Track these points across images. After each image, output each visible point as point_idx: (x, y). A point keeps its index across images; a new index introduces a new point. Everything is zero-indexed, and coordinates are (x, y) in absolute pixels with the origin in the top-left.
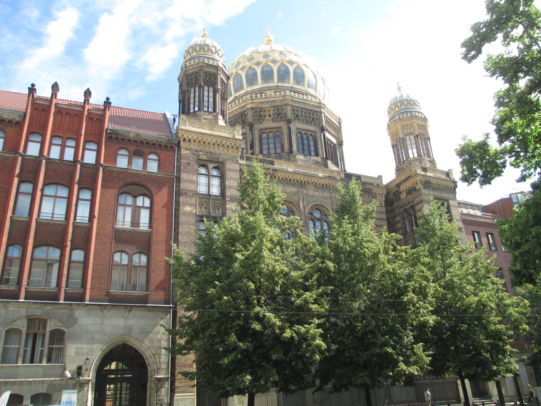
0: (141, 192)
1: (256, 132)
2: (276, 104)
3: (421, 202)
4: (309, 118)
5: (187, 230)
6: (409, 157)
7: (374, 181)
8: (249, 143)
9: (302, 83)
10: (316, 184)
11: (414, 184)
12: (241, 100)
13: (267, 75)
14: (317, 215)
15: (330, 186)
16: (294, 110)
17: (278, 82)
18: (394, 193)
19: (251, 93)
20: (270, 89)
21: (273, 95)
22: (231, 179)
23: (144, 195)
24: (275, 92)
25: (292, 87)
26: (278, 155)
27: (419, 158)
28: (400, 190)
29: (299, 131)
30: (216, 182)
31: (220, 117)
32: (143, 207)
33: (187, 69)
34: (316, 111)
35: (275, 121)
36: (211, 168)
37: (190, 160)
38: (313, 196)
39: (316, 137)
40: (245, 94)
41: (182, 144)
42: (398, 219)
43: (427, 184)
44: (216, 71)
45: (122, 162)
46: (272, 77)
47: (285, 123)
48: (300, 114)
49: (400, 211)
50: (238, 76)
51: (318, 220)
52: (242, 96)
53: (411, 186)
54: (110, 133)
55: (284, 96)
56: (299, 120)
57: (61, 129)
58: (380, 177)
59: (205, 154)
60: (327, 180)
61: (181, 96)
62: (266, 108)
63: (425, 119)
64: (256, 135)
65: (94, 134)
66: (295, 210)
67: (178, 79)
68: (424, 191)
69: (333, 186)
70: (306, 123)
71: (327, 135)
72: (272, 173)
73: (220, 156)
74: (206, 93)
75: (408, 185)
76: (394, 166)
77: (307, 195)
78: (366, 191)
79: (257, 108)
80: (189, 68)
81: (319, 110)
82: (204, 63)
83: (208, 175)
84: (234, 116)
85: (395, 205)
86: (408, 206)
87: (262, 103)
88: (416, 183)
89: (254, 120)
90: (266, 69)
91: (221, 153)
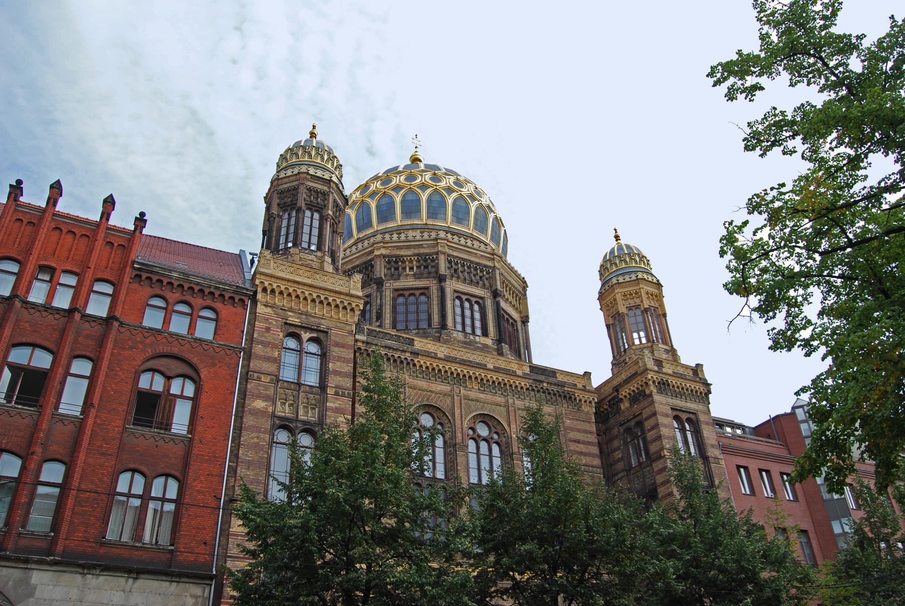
0: (180, 371)
1: (388, 293)
2: (422, 251)
4: (475, 275)
5: (256, 440)
6: (633, 343)
7: (579, 380)
8: (374, 311)
9: (466, 222)
10: (482, 379)
11: (642, 386)
12: (366, 242)
13: (411, 207)
14: (483, 431)
15: (505, 384)
16: (450, 262)
17: (428, 217)
18: (609, 401)
19: (384, 233)
20: (414, 228)
21: (418, 238)
22: (339, 359)
23: (185, 376)
24: (422, 233)
26: (421, 331)
27: (650, 344)
28: (621, 397)
29: (459, 296)
30: (313, 364)
31: (328, 259)
32: (182, 397)
34: (486, 266)
36: (305, 339)
37: (271, 323)
38: (477, 401)
39: (484, 307)
40: (374, 235)
41: (259, 296)
42: (616, 443)
43: (663, 386)
44: (326, 188)
45: (152, 319)
46: (419, 211)
47: (435, 282)
48: (461, 269)
49: (619, 431)
50: (363, 207)
51: (485, 439)
52: (368, 238)
53: (638, 389)
54: (138, 269)
55: (436, 239)
56: (458, 277)
57: (56, 256)
58: (587, 375)
61: (267, 223)
63: (659, 285)
64: (388, 299)
65: (111, 269)
66: (447, 421)
68: (657, 397)
69: (511, 386)
70: (469, 284)
71: (503, 304)
74: (307, 221)
75: (633, 386)
76: (610, 358)
79: (392, 256)
80: (284, 180)
81: (490, 264)
82: (308, 174)
83: (300, 352)
85: (612, 421)
86: (632, 423)
88: (646, 383)
89: (385, 275)
90: (410, 197)
91: (325, 317)
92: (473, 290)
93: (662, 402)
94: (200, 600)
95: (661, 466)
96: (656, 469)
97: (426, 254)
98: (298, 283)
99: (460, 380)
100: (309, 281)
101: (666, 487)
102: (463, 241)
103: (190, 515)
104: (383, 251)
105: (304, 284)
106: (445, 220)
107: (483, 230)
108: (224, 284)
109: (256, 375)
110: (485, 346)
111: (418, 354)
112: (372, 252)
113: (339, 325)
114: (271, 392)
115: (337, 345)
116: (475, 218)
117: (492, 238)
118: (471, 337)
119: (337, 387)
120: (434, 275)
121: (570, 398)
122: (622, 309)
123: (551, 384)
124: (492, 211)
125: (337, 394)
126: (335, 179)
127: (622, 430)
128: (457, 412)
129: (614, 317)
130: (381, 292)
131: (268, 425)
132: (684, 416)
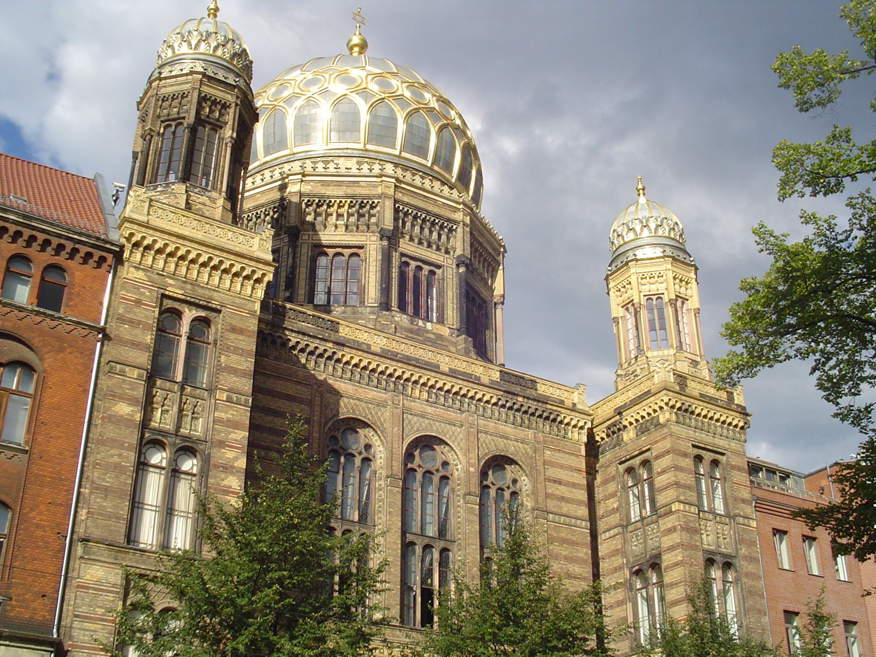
2: (358, 191)
5: (116, 459)
8: (283, 274)
16: (396, 211)
17: (369, 141)
18: (608, 428)
21: (354, 171)
22: (236, 350)
24: (358, 163)
25: (399, 157)
26: (349, 309)
28: (626, 423)
34: (449, 220)
35: (352, 231)
37: (143, 294)
39: (443, 279)
41: (126, 254)
44: (229, 97)
47: (374, 238)
53: (649, 414)
60: (460, 382)
62: (334, 197)
64: (304, 258)
66: (378, 443)
67: (139, 103)
78: (547, 418)
79: (314, 196)
84: (257, 208)
86: (637, 461)
87: (324, 183)
92: (429, 254)
95: (670, 525)
97: (364, 197)
99: (400, 383)
100: (199, 236)
101: (674, 553)
102: (418, 181)
103: (25, 558)
105: (192, 241)
107: (448, 167)
110: (440, 337)
111: (343, 345)
113: (238, 301)
114: (140, 392)
115: (233, 329)
118: (421, 323)
119: (230, 390)
121: (554, 420)
123: (528, 398)
125: (229, 400)
129: (625, 307)
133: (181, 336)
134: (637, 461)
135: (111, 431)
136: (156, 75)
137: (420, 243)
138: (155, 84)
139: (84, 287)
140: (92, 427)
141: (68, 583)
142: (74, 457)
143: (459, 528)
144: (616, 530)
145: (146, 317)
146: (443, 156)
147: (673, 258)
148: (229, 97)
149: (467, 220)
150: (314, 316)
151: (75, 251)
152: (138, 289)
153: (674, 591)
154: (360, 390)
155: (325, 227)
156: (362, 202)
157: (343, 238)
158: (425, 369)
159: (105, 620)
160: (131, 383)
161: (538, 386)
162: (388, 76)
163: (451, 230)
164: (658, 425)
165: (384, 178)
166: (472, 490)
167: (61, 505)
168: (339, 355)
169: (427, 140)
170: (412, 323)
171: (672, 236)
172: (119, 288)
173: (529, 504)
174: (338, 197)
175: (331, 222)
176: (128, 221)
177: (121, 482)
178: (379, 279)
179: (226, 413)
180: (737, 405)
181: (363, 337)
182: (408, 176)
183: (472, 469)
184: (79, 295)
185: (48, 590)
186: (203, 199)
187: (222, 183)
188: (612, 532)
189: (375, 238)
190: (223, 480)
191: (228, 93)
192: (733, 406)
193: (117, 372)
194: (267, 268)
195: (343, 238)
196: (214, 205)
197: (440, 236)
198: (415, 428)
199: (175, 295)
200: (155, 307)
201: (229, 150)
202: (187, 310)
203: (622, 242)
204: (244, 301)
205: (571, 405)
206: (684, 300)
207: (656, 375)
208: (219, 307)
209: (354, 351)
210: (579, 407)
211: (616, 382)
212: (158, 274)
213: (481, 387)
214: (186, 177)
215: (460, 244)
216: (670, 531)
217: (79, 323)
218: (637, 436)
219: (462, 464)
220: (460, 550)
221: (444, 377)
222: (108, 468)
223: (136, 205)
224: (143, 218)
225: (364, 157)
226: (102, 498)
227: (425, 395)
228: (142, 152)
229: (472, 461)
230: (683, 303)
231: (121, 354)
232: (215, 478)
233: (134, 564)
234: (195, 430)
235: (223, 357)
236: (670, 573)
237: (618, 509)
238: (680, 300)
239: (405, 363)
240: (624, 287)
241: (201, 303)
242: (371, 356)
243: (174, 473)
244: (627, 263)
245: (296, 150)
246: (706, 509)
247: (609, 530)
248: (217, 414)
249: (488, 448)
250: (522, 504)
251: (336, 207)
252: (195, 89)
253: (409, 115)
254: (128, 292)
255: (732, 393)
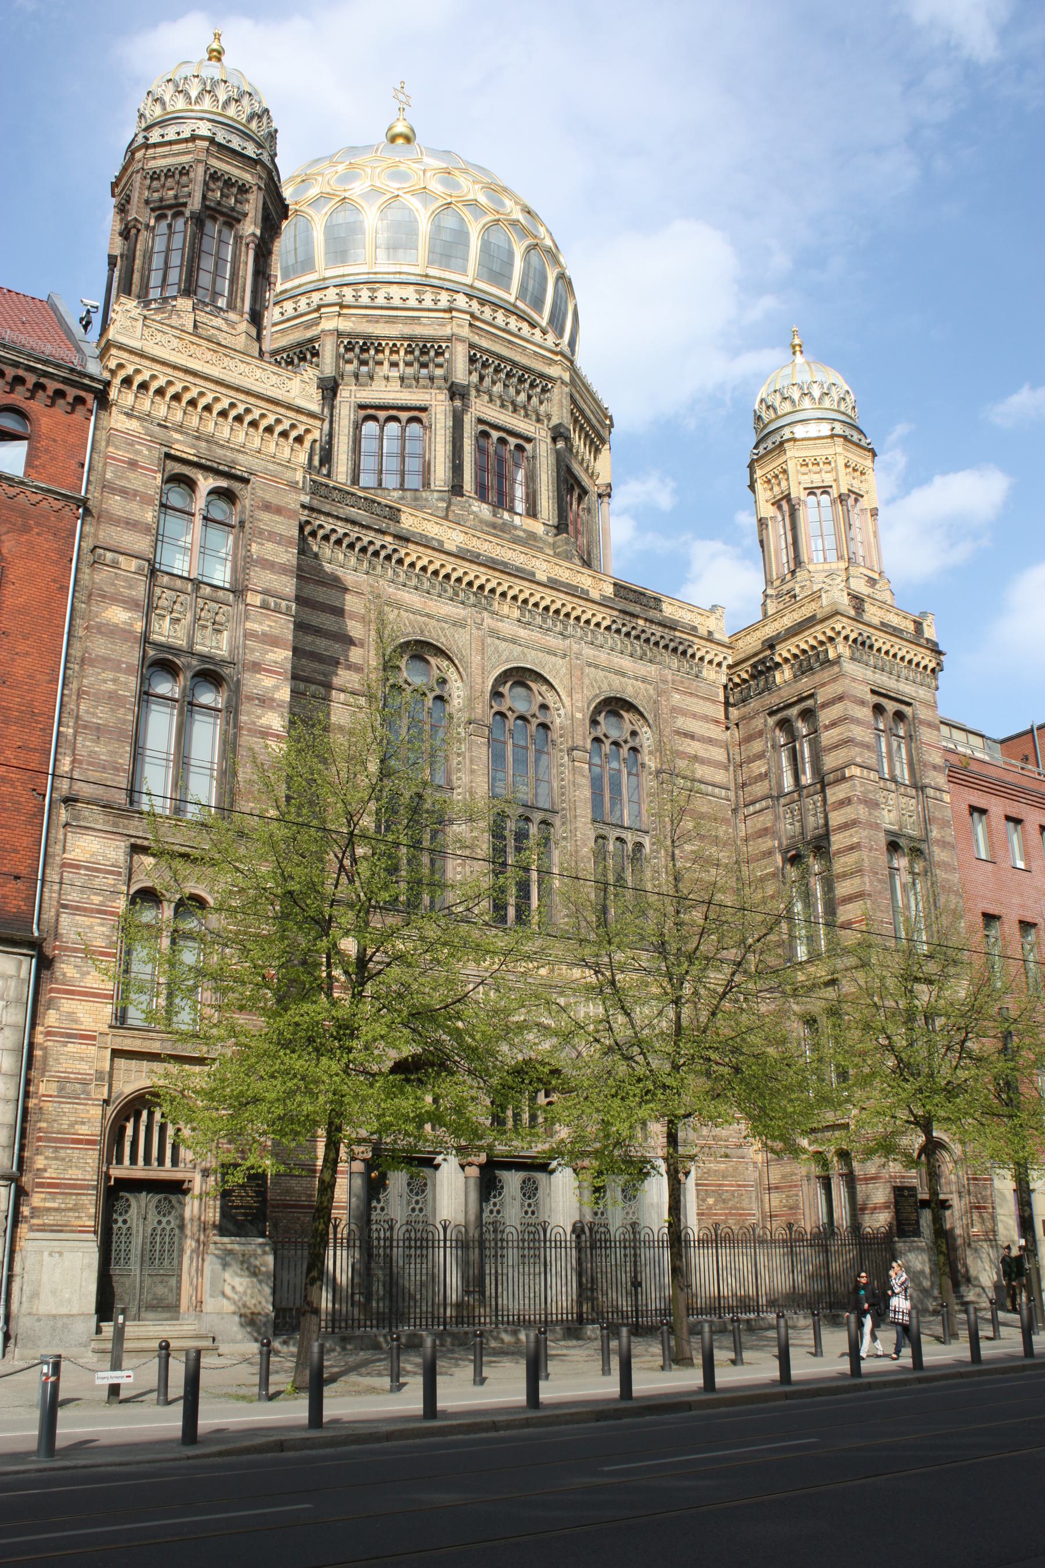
2: (418, 330)
3: (840, 698)
5: (110, 686)
16: (472, 360)
17: (430, 263)
18: (754, 666)
21: (412, 303)
25: (471, 287)
26: (408, 494)
33: (151, 151)
34: (542, 376)
35: (410, 387)
37: (138, 452)
41: (113, 394)
44: (248, 177)
55: (450, 310)
59: (190, 440)
60: (562, 596)
68: (849, 667)
72: (391, 547)
73: (241, 457)
75: (803, 642)
77: (494, 633)
79: (358, 336)
92: (515, 422)
93: (858, 677)
94: (12, 983)
95: (841, 796)
96: (831, 799)
97: (426, 339)
98: (195, 374)
100: (215, 372)
101: (847, 833)
104: (344, 325)
106: (464, 272)
107: (538, 304)
108: (46, 362)
109: (109, 555)
110: (532, 536)
111: (407, 540)
112: (316, 322)
113: (271, 467)
114: (139, 592)
115: (267, 507)
116: (525, 275)
117: (551, 321)
118: (506, 515)
119: (265, 592)
120: (441, 383)
121: (684, 653)
122: (797, 492)
123: (652, 622)
124: (556, 261)
125: (264, 606)
126: (265, 158)
127: (771, 721)
128: (476, 659)
129: (777, 504)
130: (332, 408)
131: (132, 656)
132: (891, 707)
133: (193, 515)
134: (794, 711)
135: (100, 647)
136: (140, 140)
137: (503, 406)
138: (139, 155)
139: (54, 441)
140: (74, 641)
141: (50, 860)
142: (50, 682)
143: (563, 794)
144: (764, 803)
145: (145, 485)
146: (530, 288)
147: (845, 438)
148: (248, 177)
149: (566, 377)
150: (366, 499)
151: (39, 387)
152: (132, 445)
153: (847, 883)
154: (430, 603)
155: (372, 378)
156: (425, 346)
157: (398, 395)
158: (516, 576)
159: (105, 912)
160: (126, 579)
161: (664, 606)
162: (456, 173)
163: (544, 390)
164: (827, 663)
165: (454, 314)
166: (579, 743)
167: (35, 750)
168: (403, 552)
169: (510, 264)
170: (494, 515)
171: (842, 409)
172: (104, 444)
173: (653, 765)
174: (390, 338)
175: (381, 374)
176: (116, 347)
177: (119, 719)
178: (449, 453)
179: (261, 624)
180: (927, 640)
181: (433, 529)
182: (488, 313)
183: (579, 715)
184: (47, 451)
185: (23, 871)
186: (218, 322)
187: (243, 300)
188: (758, 806)
189: (443, 396)
190: (259, 717)
191: (247, 171)
192: (923, 641)
193: (107, 562)
194: (311, 421)
195: (398, 395)
196: (234, 332)
197: (529, 397)
198: (504, 658)
199: (184, 456)
200: (155, 472)
201: (251, 253)
202: (200, 477)
203: (773, 416)
204: (281, 468)
205: (706, 633)
206: (858, 496)
207: (824, 595)
208: (246, 475)
209: (421, 549)
210: (717, 636)
211: (764, 604)
212: (159, 425)
213: (589, 605)
214: (188, 290)
215: (557, 408)
216: (846, 802)
217: (49, 491)
218: (795, 677)
219: (570, 708)
220: (563, 824)
221: (541, 589)
222: (99, 698)
223: (127, 320)
224: (136, 344)
225: (422, 284)
226: (93, 741)
227: (516, 613)
228: (122, 256)
229: (580, 704)
230: (856, 500)
231: (111, 537)
232: (248, 714)
233: (140, 834)
234: (218, 648)
235: (254, 545)
236: (842, 860)
237: (766, 774)
238: (853, 496)
239: (490, 567)
240: (776, 477)
241: (221, 467)
242: (443, 556)
243: (188, 707)
244: (782, 443)
245: (329, 273)
246: (887, 776)
247: (753, 803)
248: (249, 625)
249: (599, 688)
250: (643, 765)
251: (387, 352)
252: (199, 161)
253: (487, 229)
254: (117, 448)
255: (921, 624)
